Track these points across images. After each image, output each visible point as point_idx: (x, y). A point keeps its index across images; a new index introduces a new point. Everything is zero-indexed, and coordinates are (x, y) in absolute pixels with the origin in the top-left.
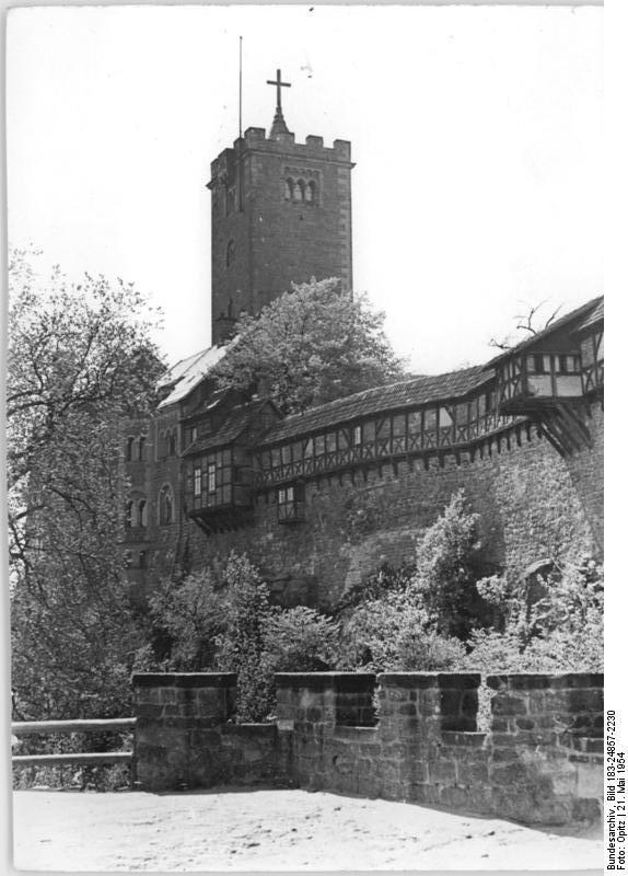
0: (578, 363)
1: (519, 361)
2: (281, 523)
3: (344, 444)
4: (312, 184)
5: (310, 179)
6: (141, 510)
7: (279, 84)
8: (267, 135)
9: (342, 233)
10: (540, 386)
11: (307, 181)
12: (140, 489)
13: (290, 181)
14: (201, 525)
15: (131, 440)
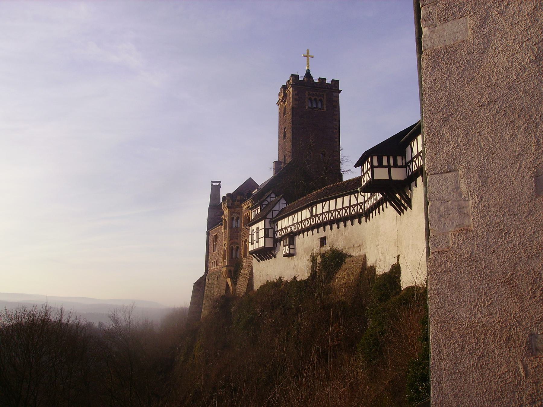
0: (404, 161)
1: (369, 159)
2: (284, 256)
3: (309, 216)
4: (321, 100)
5: (320, 98)
6: (237, 251)
7: (309, 56)
8: (301, 78)
9: (334, 122)
10: (381, 174)
11: (318, 99)
12: (235, 241)
13: (310, 99)
14: (255, 257)
15: (233, 218)
